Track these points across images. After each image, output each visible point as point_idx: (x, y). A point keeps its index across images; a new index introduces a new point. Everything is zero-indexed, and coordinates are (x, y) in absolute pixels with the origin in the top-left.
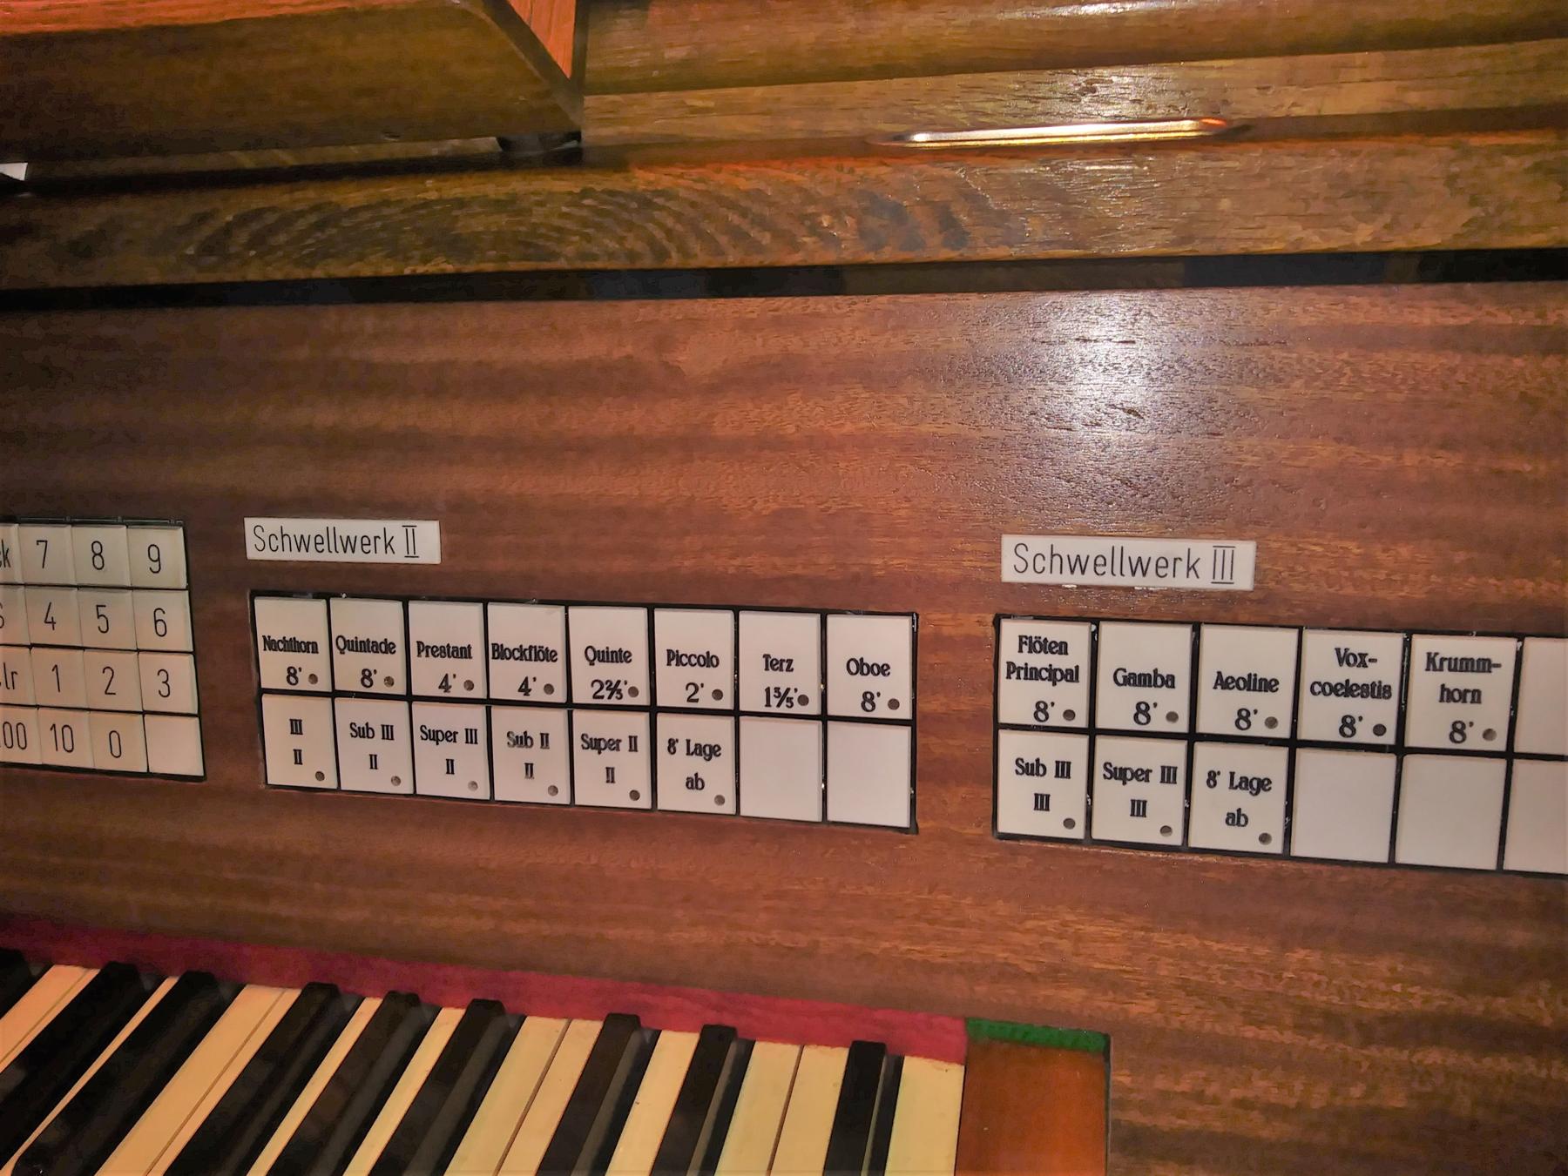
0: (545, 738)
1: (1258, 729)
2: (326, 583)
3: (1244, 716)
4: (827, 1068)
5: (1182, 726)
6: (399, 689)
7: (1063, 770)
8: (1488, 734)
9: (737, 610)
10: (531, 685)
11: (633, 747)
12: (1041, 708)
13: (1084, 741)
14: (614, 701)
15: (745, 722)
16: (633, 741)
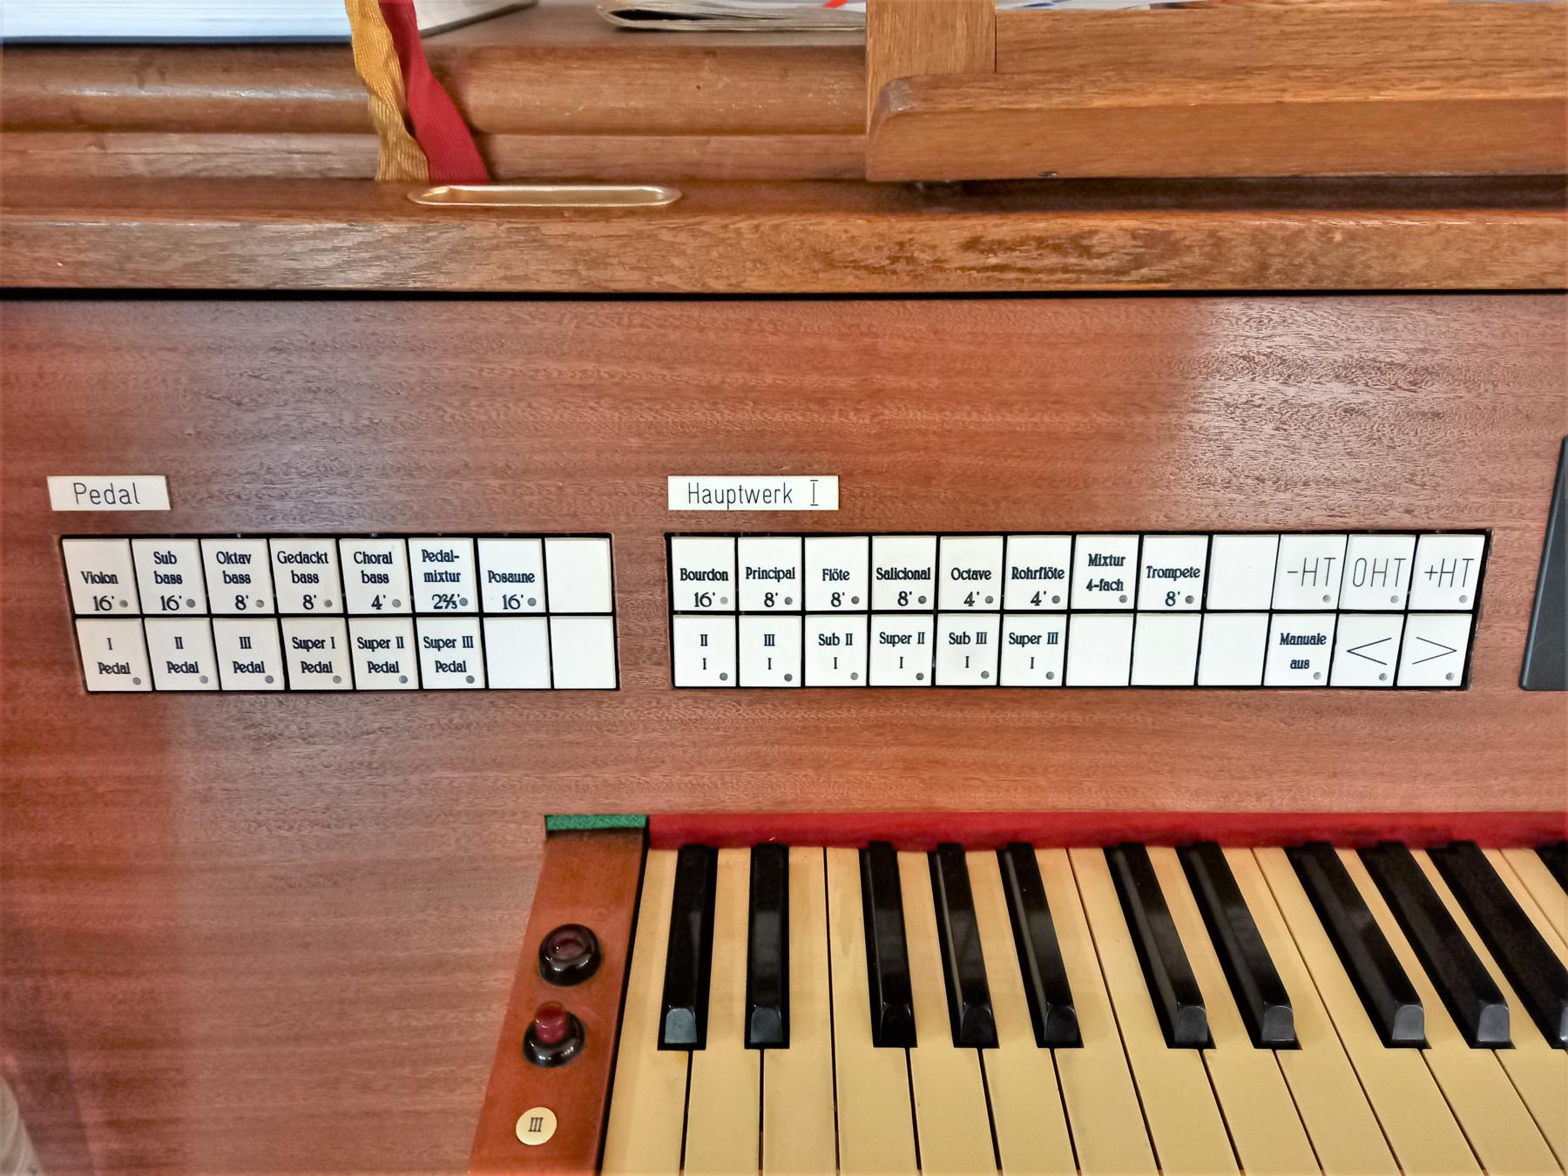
0: (849, 637)
1: (913, 604)
2: (736, 528)
3: (903, 597)
4: (845, 865)
5: (929, 605)
6: (540, 608)
7: (982, 638)
8: (1189, 599)
9: (1005, 535)
10: (975, 597)
11: (921, 641)
12: (769, 598)
13: (930, 618)
14: (450, 610)
15: (742, 619)
16: (921, 636)
